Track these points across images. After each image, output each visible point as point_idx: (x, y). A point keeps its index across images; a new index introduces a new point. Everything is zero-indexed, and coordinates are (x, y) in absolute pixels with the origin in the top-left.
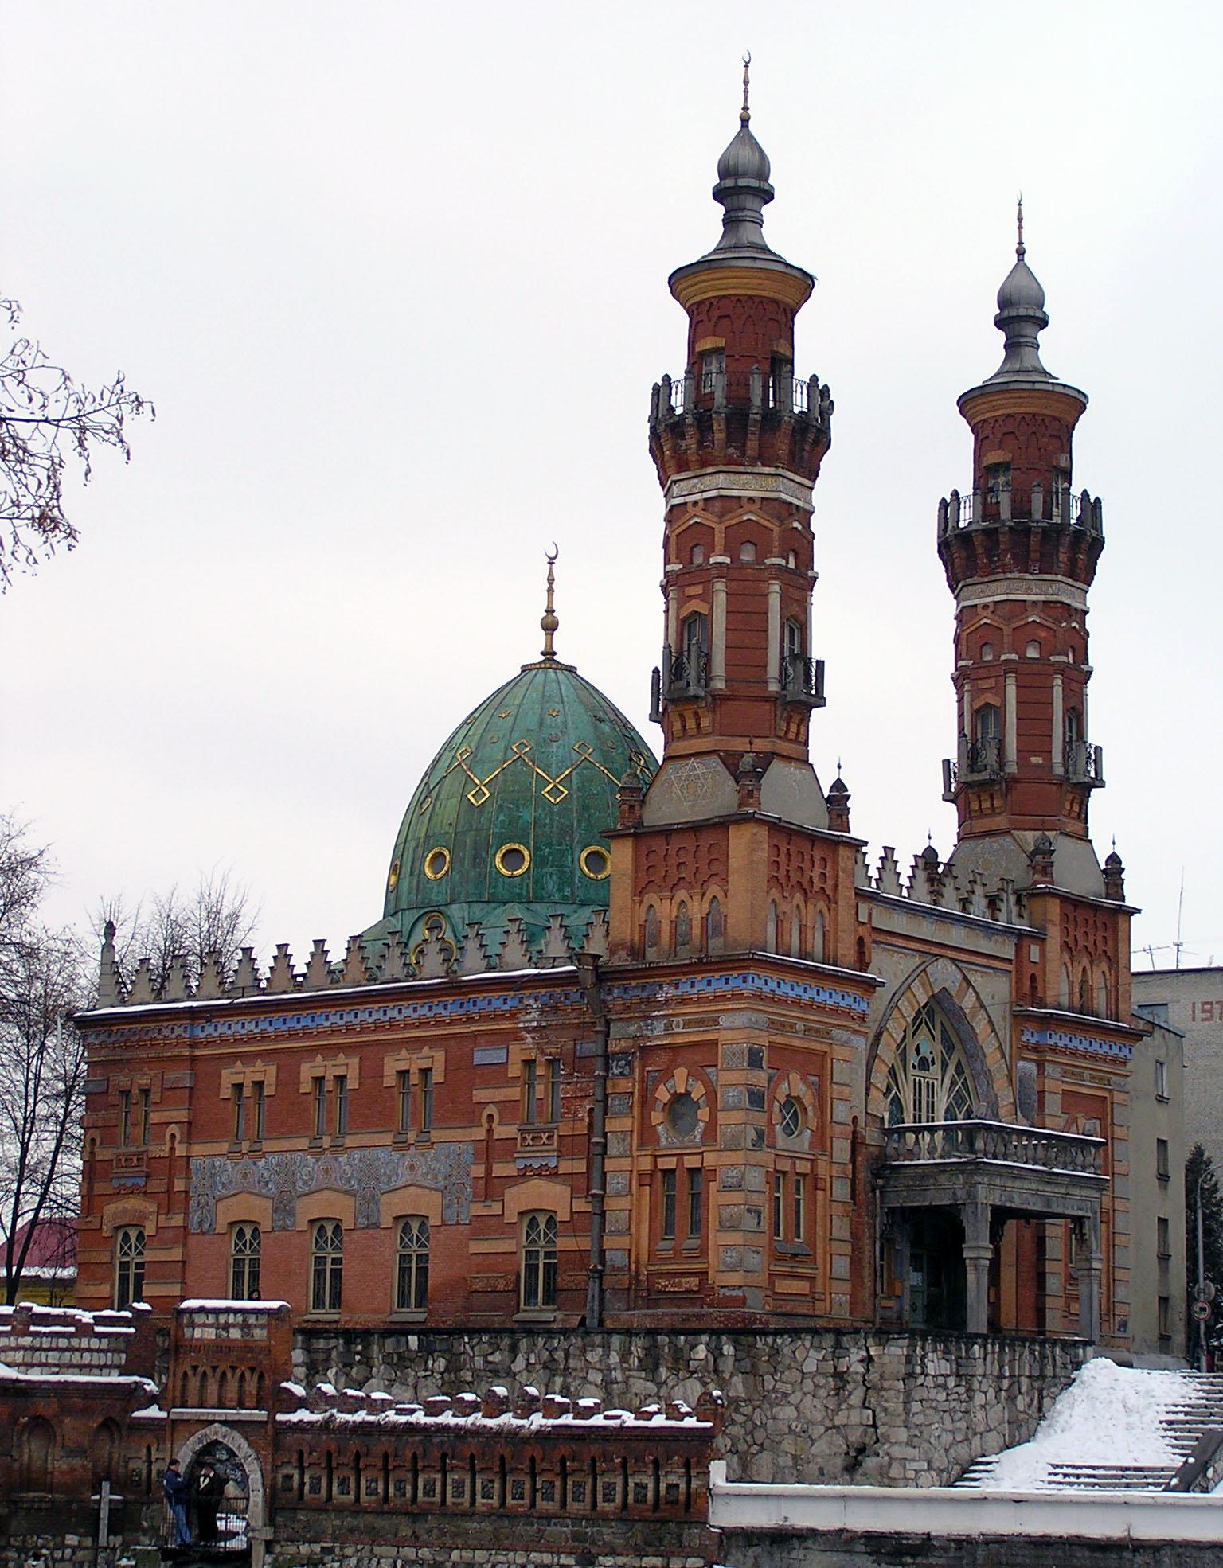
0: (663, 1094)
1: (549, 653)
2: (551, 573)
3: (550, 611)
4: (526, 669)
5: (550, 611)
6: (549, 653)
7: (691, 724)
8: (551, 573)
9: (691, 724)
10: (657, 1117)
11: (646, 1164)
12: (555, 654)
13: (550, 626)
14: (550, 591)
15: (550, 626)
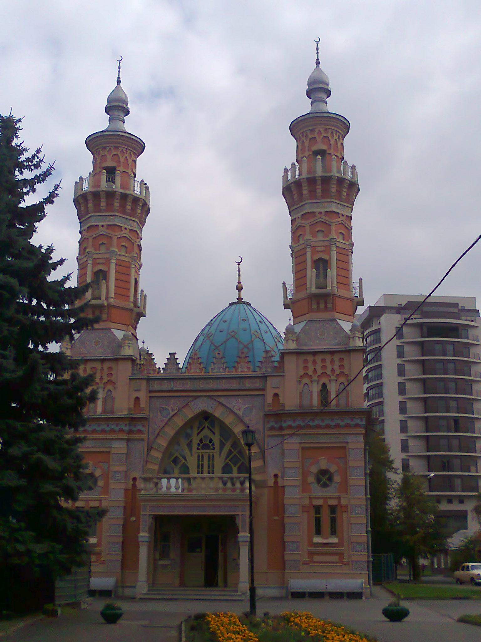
0: (314, 469)
1: (240, 299)
2: (239, 268)
3: (239, 282)
4: (231, 304)
5: (239, 282)
6: (240, 299)
7: (322, 306)
8: (239, 268)
9: (322, 306)
10: (311, 479)
11: (307, 502)
12: (242, 299)
13: (239, 289)
14: (239, 275)
15: (239, 289)
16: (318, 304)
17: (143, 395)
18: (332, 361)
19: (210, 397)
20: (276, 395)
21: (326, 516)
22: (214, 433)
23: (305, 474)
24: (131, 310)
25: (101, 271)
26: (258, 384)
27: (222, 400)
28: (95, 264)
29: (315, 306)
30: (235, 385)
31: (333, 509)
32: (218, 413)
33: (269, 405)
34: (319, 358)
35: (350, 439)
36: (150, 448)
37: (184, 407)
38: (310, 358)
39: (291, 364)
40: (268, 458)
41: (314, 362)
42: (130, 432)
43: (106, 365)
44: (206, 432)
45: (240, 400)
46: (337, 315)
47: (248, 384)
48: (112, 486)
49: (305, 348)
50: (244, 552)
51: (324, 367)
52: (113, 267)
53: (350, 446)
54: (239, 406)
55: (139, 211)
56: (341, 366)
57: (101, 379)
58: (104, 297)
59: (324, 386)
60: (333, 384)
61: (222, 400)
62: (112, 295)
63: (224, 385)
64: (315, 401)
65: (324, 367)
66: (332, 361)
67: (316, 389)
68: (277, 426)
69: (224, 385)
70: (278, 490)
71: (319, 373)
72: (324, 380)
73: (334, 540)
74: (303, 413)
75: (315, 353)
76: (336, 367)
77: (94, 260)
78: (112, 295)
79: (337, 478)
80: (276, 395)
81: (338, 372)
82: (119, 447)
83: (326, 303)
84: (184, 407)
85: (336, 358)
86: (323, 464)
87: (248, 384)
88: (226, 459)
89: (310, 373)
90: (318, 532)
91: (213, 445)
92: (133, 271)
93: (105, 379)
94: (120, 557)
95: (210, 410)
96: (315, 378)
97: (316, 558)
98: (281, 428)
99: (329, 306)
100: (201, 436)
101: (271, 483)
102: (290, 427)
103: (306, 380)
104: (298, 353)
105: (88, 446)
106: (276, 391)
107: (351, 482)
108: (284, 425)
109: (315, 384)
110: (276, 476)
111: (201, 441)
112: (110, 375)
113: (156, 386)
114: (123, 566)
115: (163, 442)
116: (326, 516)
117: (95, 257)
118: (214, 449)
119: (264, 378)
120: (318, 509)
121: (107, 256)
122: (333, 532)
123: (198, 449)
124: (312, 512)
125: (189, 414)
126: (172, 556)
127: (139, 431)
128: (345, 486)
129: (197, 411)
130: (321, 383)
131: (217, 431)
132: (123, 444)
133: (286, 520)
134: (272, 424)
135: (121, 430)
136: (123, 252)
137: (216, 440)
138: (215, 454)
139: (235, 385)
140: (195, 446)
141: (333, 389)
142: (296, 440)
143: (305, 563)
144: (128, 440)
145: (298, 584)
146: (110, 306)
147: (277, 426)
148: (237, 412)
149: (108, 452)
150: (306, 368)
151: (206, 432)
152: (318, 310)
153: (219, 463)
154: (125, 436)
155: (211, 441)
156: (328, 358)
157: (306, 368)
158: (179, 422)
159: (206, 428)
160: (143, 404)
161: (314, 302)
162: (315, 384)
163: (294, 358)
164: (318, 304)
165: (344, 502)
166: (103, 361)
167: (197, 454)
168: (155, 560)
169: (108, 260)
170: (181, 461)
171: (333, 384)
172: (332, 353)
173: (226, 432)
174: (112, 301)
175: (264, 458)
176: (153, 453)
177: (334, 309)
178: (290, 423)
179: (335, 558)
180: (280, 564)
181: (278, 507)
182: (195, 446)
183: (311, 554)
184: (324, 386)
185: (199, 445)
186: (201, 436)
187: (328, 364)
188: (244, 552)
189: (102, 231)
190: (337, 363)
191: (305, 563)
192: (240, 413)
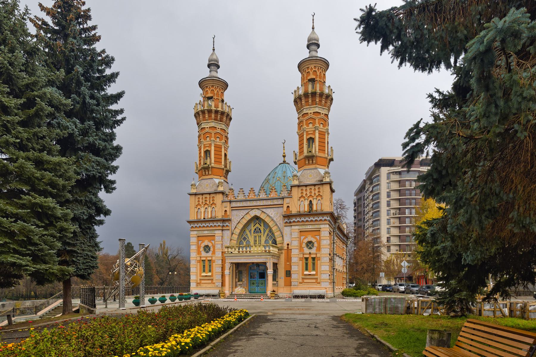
0: (306, 241)
7: (311, 162)
9: (311, 162)
16: (309, 161)
17: (228, 209)
18: (315, 189)
19: (258, 209)
20: (288, 207)
21: (310, 261)
23: (301, 244)
24: (223, 169)
25: (207, 150)
26: (280, 202)
27: (264, 210)
28: (205, 147)
29: (307, 162)
30: (269, 203)
31: (314, 259)
32: (263, 216)
33: (285, 212)
34: (308, 188)
35: (322, 226)
38: (304, 188)
39: (296, 192)
40: (285, 237)
41: (306, 190)
42: (223, 226)
43: (212, 195)
44: (257, 225)
45: (272, 210)
46: (318, 166)
47: (276, 202)
48: (216, 251)
49: (302, 184)
50: (270, 278)
51: (311, 192)
52: (213, 148)
53: (321, 230)
54: (271, 212)
55: (225, 119)
56: (319, 191)
57: (210, 202)
58: (208, 163)
59: (311, 201)
60: (315, 200)
61: (264, 210)
62: (213, 161)
63: (265, 203)
64: (306, 209)
65: (311, 192)
66: (315, 189)
67: (307, 203)
68: (288, 221)
69: (265, 203)
70: (289, 250)
71: (308, 195)
72: (311, 199)
73: (314, 273)
74: (300, 215)
75: (306, 186)
76: (316, 192)
77: (204, 145)
78: (213, 161)
79: (316, 245)
80: (288, 207)
81: (317, 194)
82: (218, 233)
83: (312, 161)
85: (317, 187)
86: (310, 238)
87: (276, 202)
89: (304, 195)
90: (307, 269)
92: (223, 149)
93: (212, 202)
94: (221, 281)
96: (306, 198)
97: (305, 281)
98: (290, 222)
99: (314, 162)
100: (255, 227)
101: (286, 248)
102: (294, 222)
103: (302, 199)
104: (299, 186)
106: (288, 205)
107: (322, 247)
108: (292, 221)
109: (306, 200)
110: (288, 244)
111: (255, 229)
113: (234, 204)
114: (222, 286)
115: (237, 231)
116: (310, 261)
117: (205, 143)
119: (283, 198)
120: (307, 259)
121: (210, 143)
122: (314, 269)
124: (304, 260)
125: (248, 218)
126: (243, 280)
127: (227, 226)
128: (319, 249)
129: (252, 215)
130: (309, 200)
131: (262, 225)
132: (220, 232)
133: (292, 264)
134: (286, 220)
135: (219, 226)
136: (218, 140)
139: (269, 203)
140: (252, 232)
141: (314, 202)
142: (297, 227)
143: (300, 283)
144: (222, 230)
145: (297, 292)
146: (212, 167)
147: (288, 221)
150: (302, 193)
151: (257, 225)
152: (309, 164)
153: (263, 239)
154: (221, 228)
155: (260, 229)
156: (313, 187)
157: (302, 193)
158: (244, 222)
160: (228, 213)
161: (307, 160)
162: (306, 200)
163: (296, 188)
164: (309, 161)
165: (318, 256)
166: (210, 194)
168: (236, 282)
169: (210, 144)
171: (315, 200)
172: (315, 185)
173: (266, 224)
174: (213, 165)
175: (283, 236)
176: (234, 235)
177: (316, 164)
178: (294, 220)
179: (314, 281)
180: (289, 284)
181: (289, 259)
182: (252, 232)
183: (303, 279)
184: (311, 201)
186: (255, 227)
187: (313, 191)
188: (270, 278)
189: (207, 130)
190: (317, 190)
191: (300, 283)
192: (272, 216)
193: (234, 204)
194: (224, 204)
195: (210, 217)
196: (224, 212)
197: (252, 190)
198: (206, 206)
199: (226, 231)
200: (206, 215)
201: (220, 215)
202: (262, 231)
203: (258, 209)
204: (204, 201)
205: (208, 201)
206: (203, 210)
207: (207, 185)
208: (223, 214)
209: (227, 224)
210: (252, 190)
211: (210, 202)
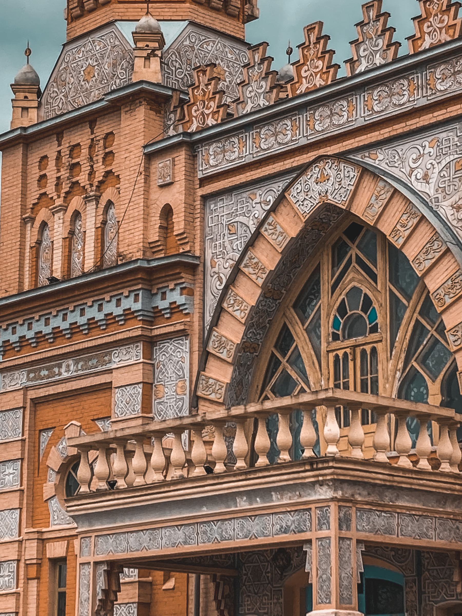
17: (176, 197)
22: (374, 277)
27: (379, 159)
36: (205, 356)
37: (274, 209)
42: (153, 316)
43: (102, 129)
44: (354, 279)
45: (426, 144)
57: (92, 173)
82: (126, 364)
84: (274, 209)
88: (407, 361)
91: (373, 317)
95: (339, 200)
105: (65, 375)
111: (342, 310)
112: (109, 156)
118: (374, 329)
123: (336, 337)
127: (175, 309)
131: (381, 268)
135: (129, 315)
137: (380, 294)
138: (379, 347)
140: (325, 329)
148: (418, 186)
149: (107, 387)
151: (354, 279)
155: (368, 303)
159: (354, 264)
166: (90, 119)
167: (331, 356)
170: (296, 384)
182: (325, 329)
185: (336, 324)
192: (429, 189)
193: (213, 159)
194: (159, 165)
195: (89, 265)
196: (156, 221)
197: (317, 35)
198: (76, 202)
199: (170, 347)
200: (76, 259)
201: (133, 238)
202: (383, 318)
203: (342, 157)
204: (64, 173)
205: (86, 168)
206: (59, 228)
207: (89, 71)
208: (154, 236)
209: (176, 297)
210: (317, 35)
211: (92, 173)
